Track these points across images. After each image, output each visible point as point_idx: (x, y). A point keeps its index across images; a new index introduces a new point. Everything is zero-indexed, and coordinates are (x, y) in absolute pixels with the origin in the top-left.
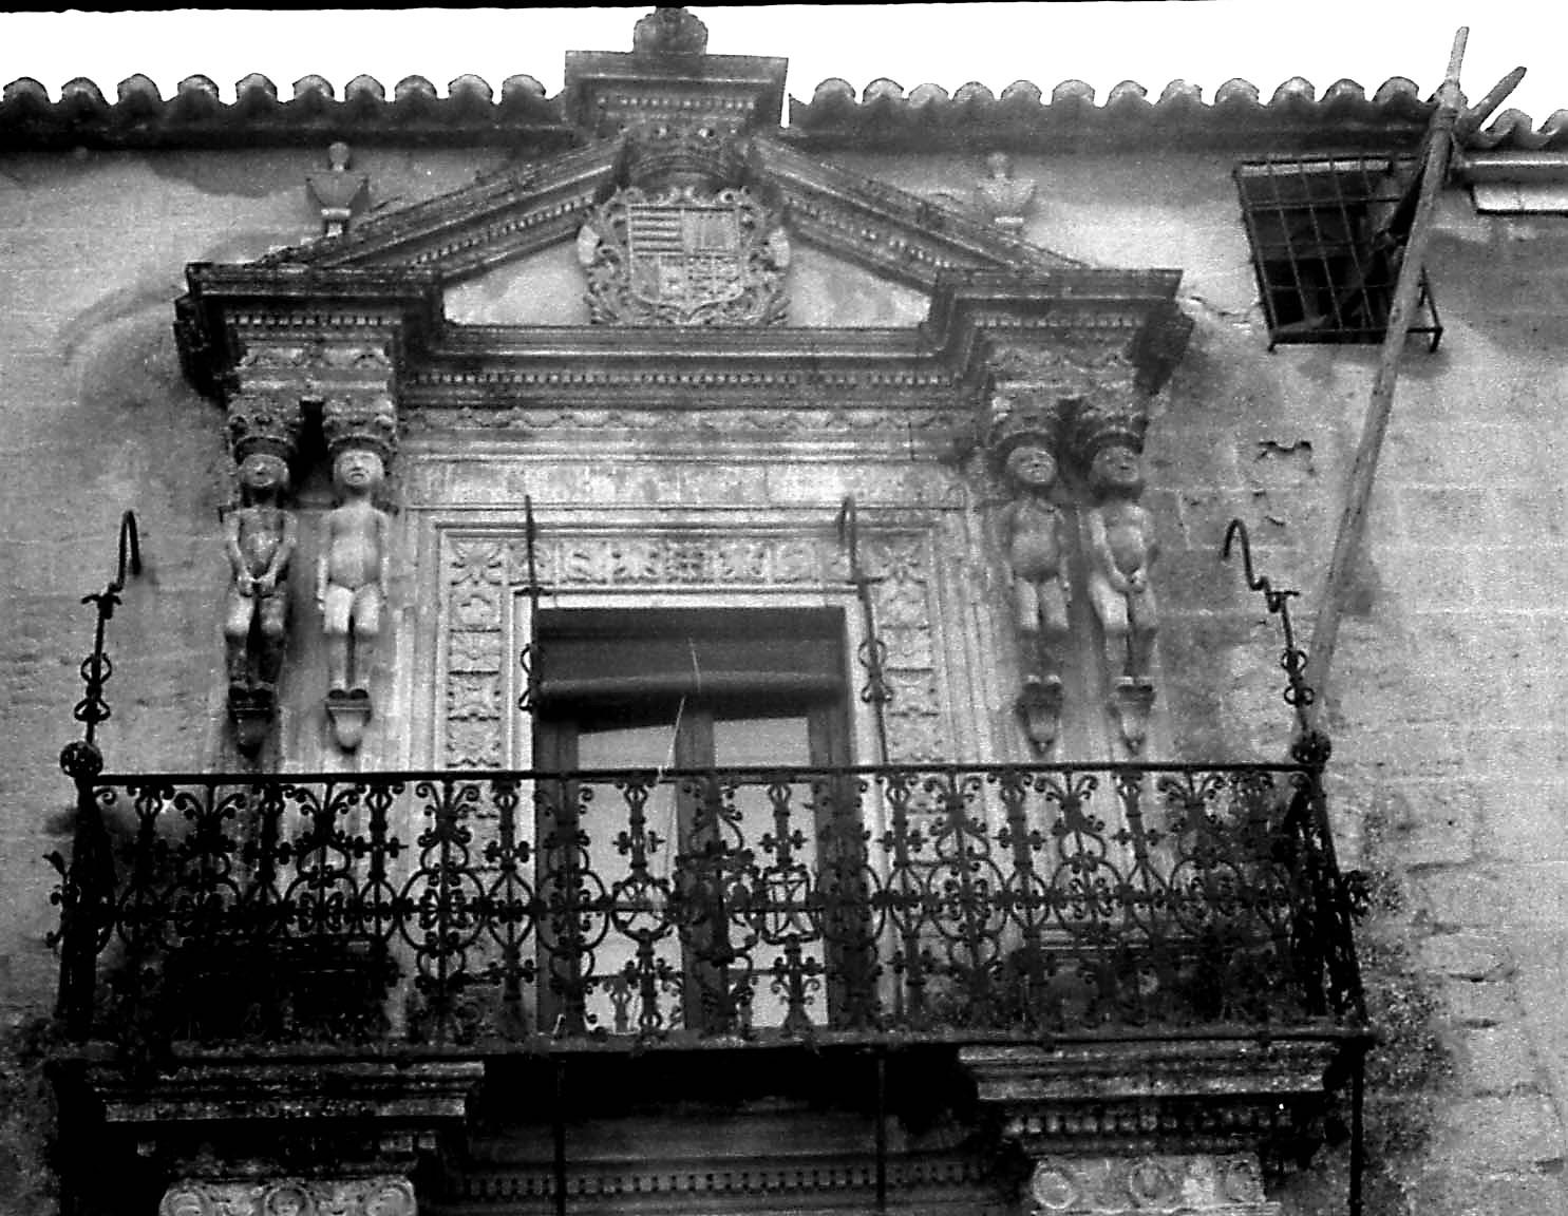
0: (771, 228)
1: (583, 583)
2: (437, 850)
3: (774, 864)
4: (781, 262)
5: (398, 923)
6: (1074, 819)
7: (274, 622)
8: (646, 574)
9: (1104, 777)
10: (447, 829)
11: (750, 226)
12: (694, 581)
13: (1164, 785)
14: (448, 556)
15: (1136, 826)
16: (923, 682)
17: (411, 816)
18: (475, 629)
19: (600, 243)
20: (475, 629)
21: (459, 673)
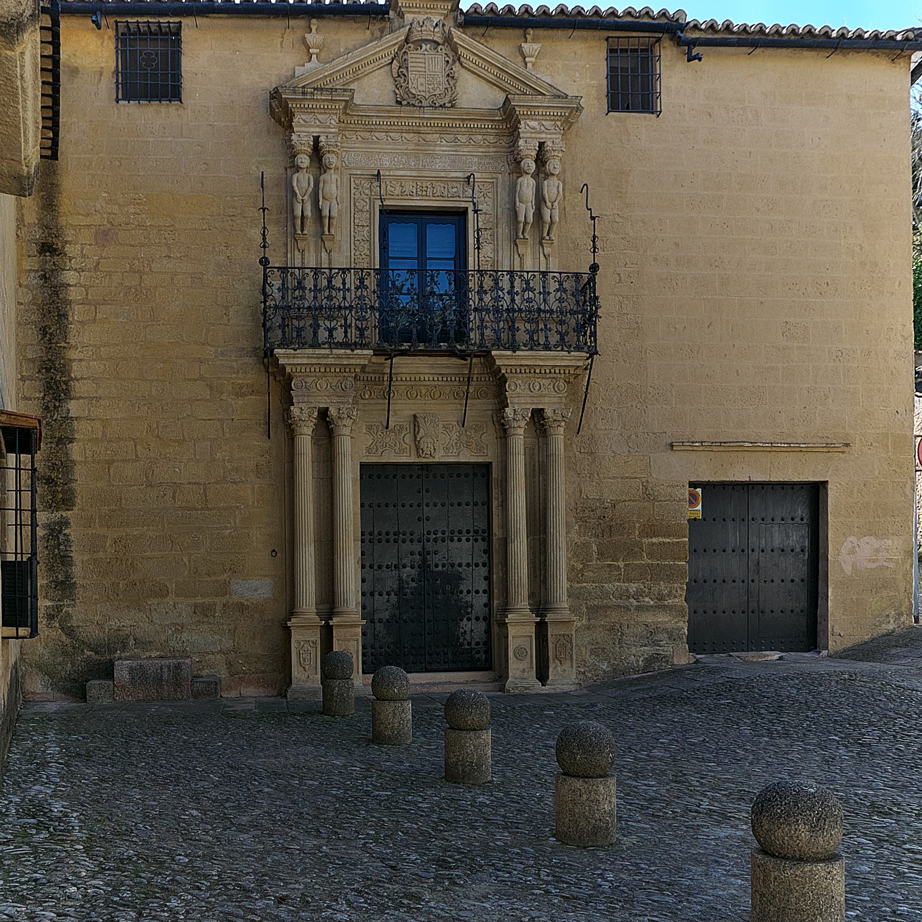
5: (350, 312)
10: (361, 285)
11: (448, 62)
17: (351, 280)
19: (400, 67)
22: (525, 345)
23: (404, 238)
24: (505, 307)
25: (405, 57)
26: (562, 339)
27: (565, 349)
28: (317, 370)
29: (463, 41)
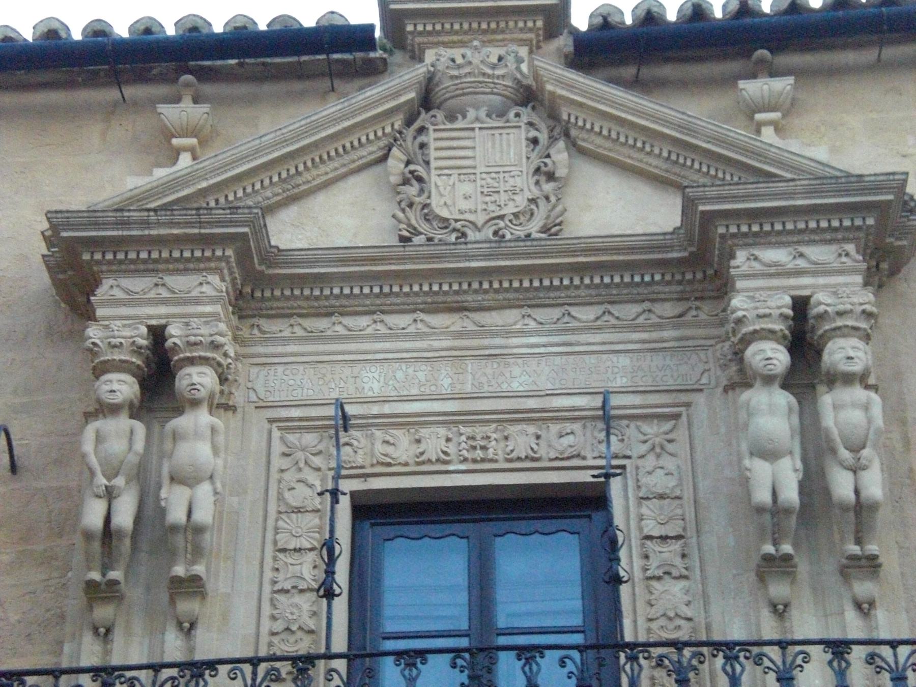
0: (553, 140)
1: (387, 466)
4: (561, 172)
8: (443, 456)
9: (815, 651)
11: (535, 141)
12: (483, 460)
13: (871, 659)
14: (278, 447)
16: (676, 546)
18: (298, 510)
19: (408, 163)
20: (298, 510)
21: (284, 550)
23: (425, 583)
25: (422, 138)
29: (570, 87)
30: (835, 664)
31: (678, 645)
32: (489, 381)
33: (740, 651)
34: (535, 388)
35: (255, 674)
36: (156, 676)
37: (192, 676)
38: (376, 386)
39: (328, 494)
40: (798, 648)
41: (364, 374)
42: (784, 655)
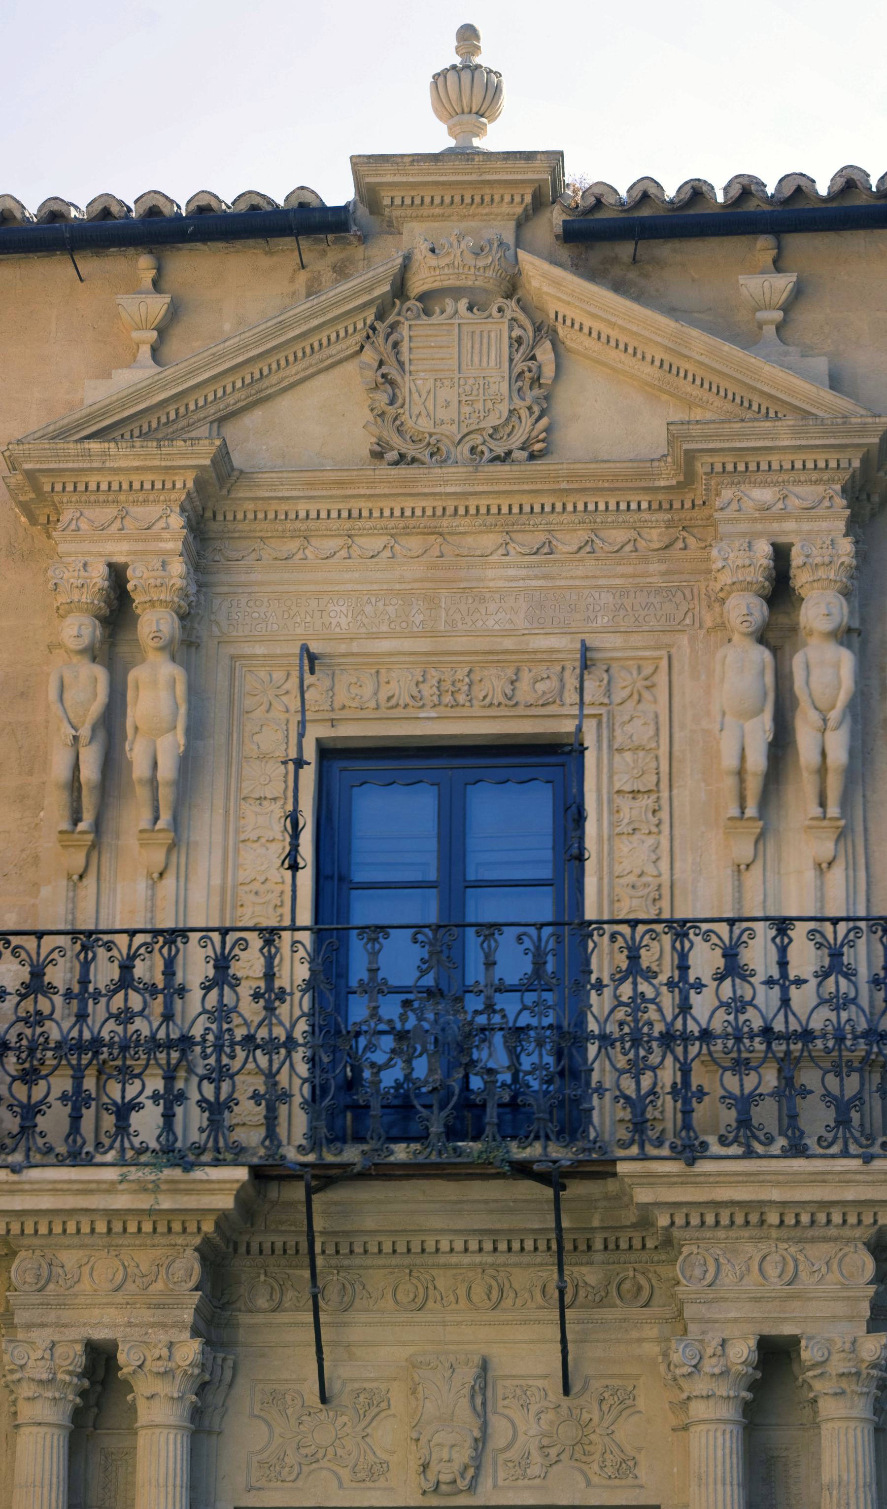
2: (214, 994)
3: (481, 1007)
6: (732, 967)
7: (89, 772)
9: (759, 927)
11: (519, 341)
15: (784, 974)
16: (648, 802)
22: (723, 1141)
23: (396, 826)
24: (659, 1028)
26: (843, 1121)
27: (853, 1149)
28: (85, 1229)
30: (778, 940)
31: (634, 923)
32: (463, 619)
33: (690, 928)
34: (512, 627)
35: (223, 943)
36: (131, 941)
37: (165, 944)
38: (344, 621)
39: (291, 763)
40: (745, 925)
41: (331, 607)
42: (731, 931)
